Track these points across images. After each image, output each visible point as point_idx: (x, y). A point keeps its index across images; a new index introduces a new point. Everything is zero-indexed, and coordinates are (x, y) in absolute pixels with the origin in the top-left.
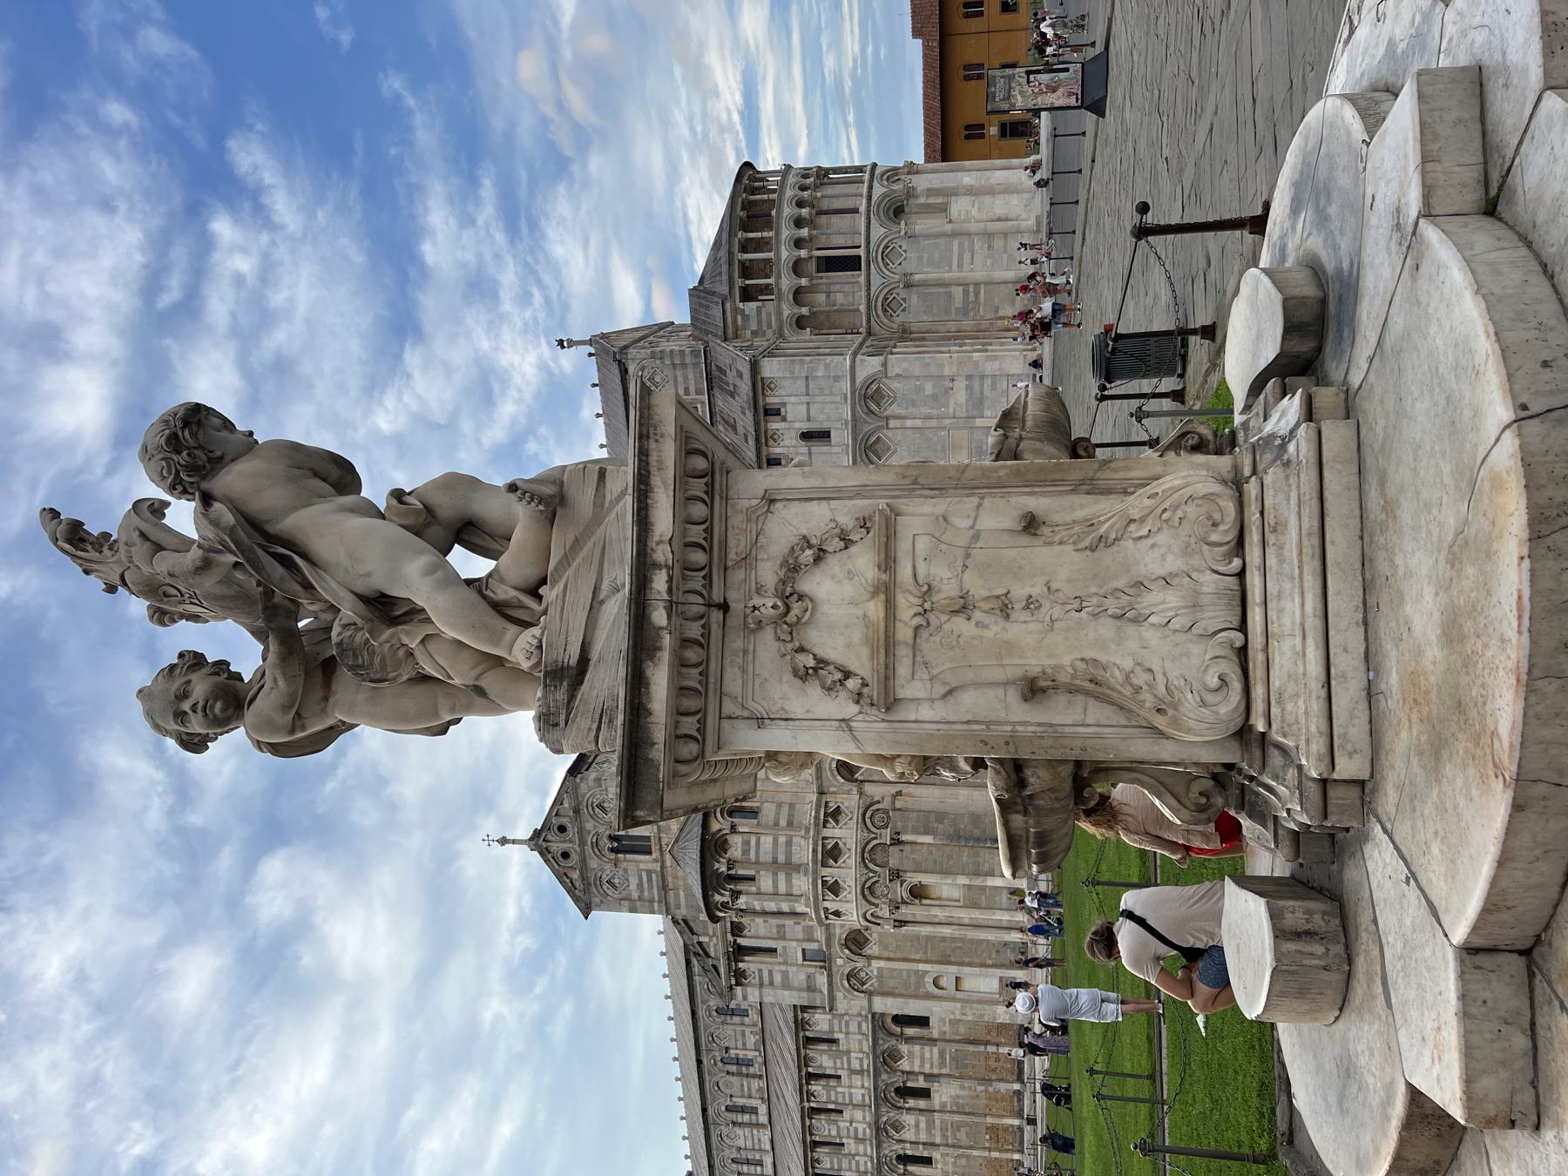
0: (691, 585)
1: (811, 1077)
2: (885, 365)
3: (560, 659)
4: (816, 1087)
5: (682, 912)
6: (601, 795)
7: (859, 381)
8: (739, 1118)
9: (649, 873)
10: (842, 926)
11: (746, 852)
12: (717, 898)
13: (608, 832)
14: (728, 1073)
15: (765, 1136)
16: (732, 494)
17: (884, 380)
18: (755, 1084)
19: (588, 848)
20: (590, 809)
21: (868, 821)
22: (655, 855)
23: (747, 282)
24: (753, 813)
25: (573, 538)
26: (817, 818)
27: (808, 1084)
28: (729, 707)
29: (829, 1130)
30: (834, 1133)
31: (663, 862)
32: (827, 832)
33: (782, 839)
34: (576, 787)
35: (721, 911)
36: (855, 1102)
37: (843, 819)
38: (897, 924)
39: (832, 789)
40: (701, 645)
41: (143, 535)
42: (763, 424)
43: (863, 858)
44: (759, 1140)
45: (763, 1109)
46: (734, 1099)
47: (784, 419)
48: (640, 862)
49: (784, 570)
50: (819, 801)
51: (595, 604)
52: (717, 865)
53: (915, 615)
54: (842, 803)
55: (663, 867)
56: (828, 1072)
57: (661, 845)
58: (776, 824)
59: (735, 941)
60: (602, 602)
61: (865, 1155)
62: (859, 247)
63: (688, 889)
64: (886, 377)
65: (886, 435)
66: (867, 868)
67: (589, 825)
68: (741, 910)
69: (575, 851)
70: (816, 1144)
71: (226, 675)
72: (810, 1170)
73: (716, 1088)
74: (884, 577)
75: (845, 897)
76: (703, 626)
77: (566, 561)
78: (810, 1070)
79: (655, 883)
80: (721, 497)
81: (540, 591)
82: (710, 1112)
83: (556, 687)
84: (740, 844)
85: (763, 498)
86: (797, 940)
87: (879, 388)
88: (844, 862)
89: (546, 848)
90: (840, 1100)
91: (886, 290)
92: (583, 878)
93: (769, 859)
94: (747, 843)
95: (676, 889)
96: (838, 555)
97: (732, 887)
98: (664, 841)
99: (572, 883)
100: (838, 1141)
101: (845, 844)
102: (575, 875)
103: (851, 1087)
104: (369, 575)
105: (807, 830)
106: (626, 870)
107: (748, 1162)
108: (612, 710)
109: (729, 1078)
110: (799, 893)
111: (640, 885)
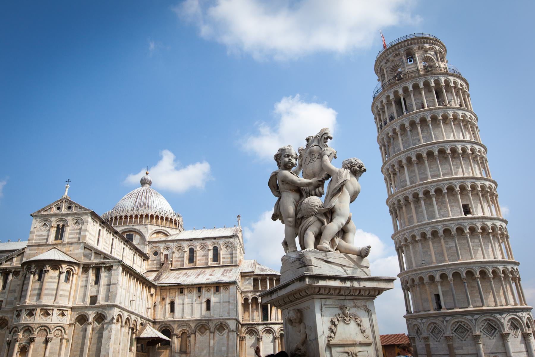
0: (352, 291)
2: (233, 331)
5: (27, 251)
7: (228, 322)
11: (51, 278)
12: (33, 266)
16: (369, 301)
17: (227, 331)
19: (61, 217)
20: (76, 218)
21: (58, 328)
23: (259, 280)
24: (67, 280)
26: (62, 307)
32: (55, 310)
34: (86, 214)
35: (27, 267)
37: (60, 317)
38: (9, 341)
40: (338, 294)
42: (213, 286)
43: (42, 326)
47: (214, 293)
52: (47, 266)
53: (351, 352)
59: (11, 272)
60: (342, 267)
62: (271, 321)
63: (37, 254)
64: (229, 332)
65: (208, 333)
66: (38, 328)
68: (26, 276)
74: (358, 344)
79: (42, 241)
86: (7, 298)
87: (225, 329)
88: (42, 318)
91: (257, 331)
94: (55, 278)
96: (360, 330)
97: (37, 272)
99: (47, 210)
111: (42, 235)
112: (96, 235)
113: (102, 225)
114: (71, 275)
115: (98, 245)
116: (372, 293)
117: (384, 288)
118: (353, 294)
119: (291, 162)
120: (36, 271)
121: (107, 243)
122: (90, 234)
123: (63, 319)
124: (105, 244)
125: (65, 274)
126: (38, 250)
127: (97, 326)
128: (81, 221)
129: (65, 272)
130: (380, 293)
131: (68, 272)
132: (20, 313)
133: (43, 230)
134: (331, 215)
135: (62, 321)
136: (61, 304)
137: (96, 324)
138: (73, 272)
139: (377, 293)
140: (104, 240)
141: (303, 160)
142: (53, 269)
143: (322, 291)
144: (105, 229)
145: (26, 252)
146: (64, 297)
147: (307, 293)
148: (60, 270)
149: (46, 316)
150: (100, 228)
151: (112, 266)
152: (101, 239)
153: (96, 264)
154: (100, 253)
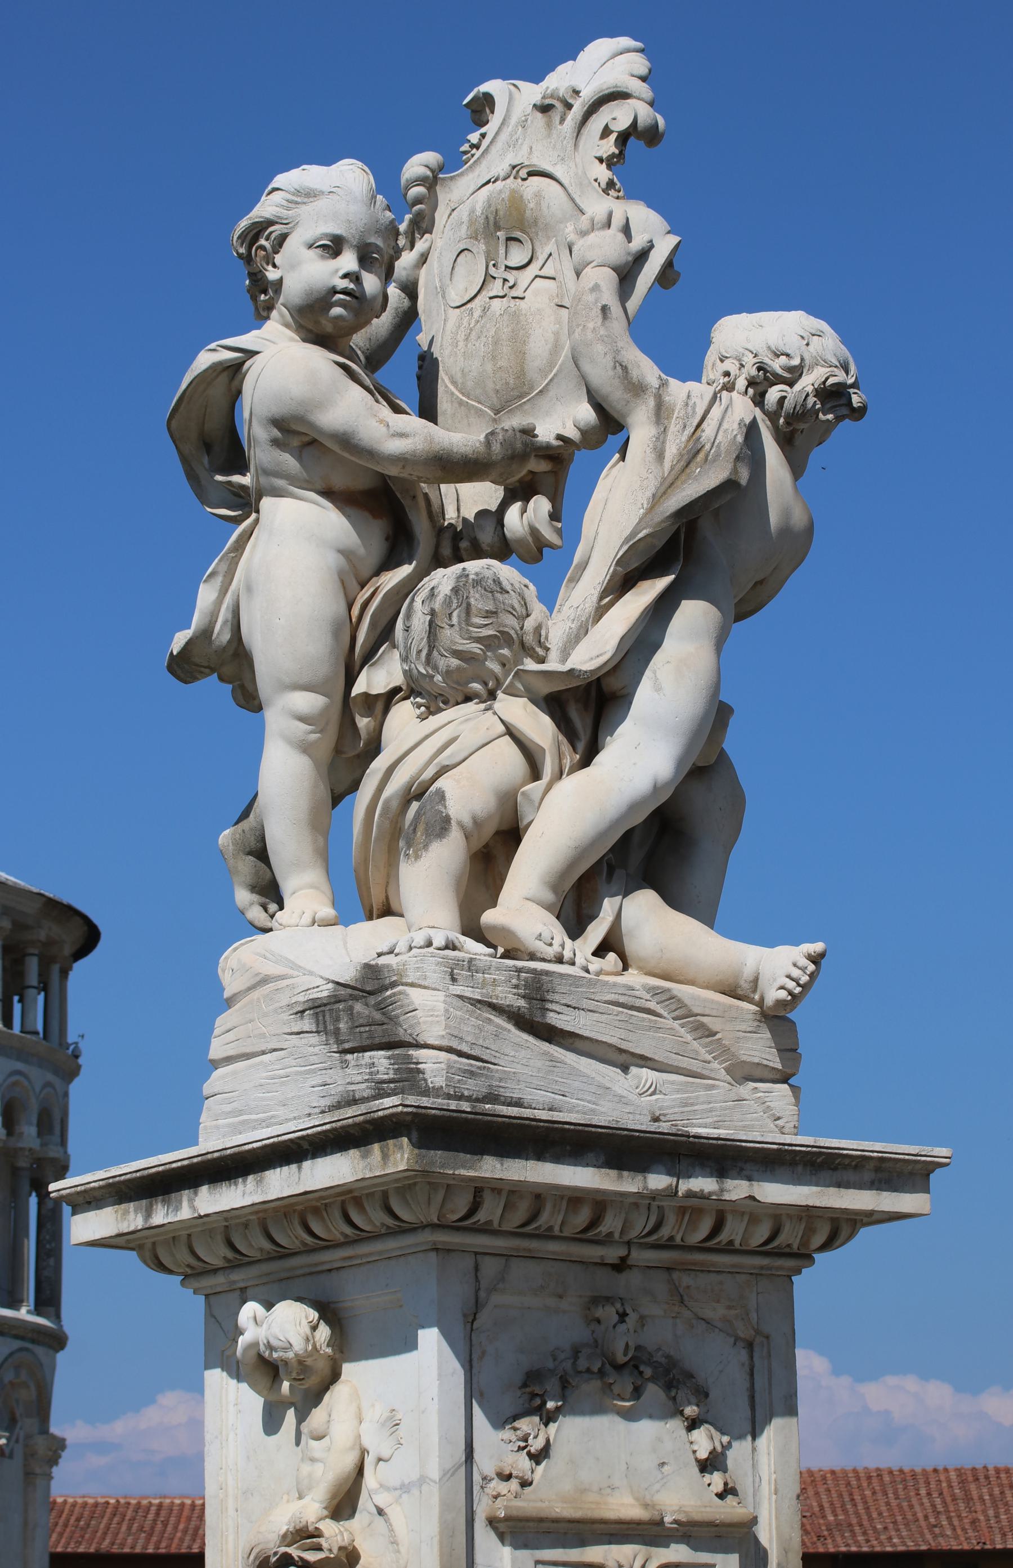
0: (671, 1219)
3: (556, 997)
25: (715, 1028)
28: (490, 1267)
40: (585, 1230)
49: (663, 1360)
51: (622, 1058)
60: (625, 1069)
76: (610, 1234)
77: (684, 1013)
80: (762, 1268)
83: (516, 987)
85: (758, 1332)
108: (487, 1077)
116: (790, 1236)
117: (870, 1213)
118: (671, 1238)
130: (844, 1233)
134: (589, 721)
139: (818, 1240)
141: (433, 258)
143: (490, 1211)
147: (396, 1217)
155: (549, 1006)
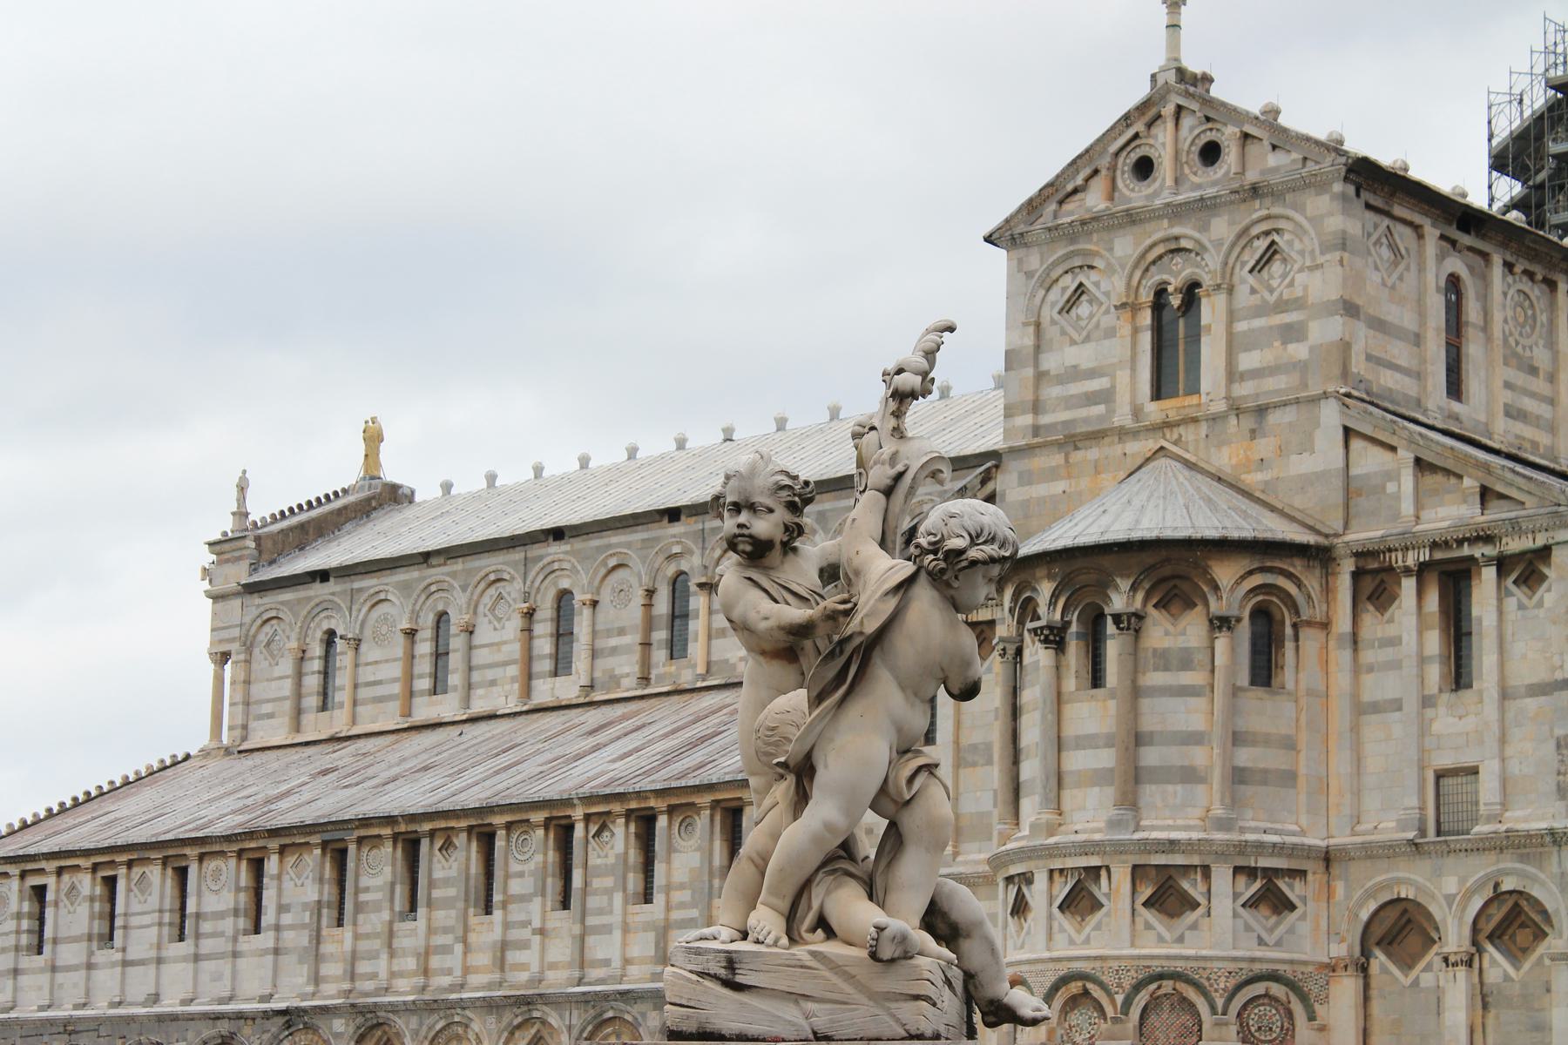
1: (645, 823)
4: (621, 838)
6: (1302, 253)
8: (544, 629)
9: (1106, 397)
10: (993, 917)
11: (1165, 661)
12: (1045, 589)
13: (1207, 281)
14: (650, 593)
15: (504, 698)
18: (627, 667)
19: (1163, 229)
20: (1264, 227)
21: (1258, 989)
22: (1155, 411)
24: (1264, 671)
26: (1260, 847)
27: (628, 815)
29: (521, 875)
30: (515, 887)
31: (1134, 434)
32: (1222, 877)
33: (1199, 756)
34: (1316, 184)
36: (591, 940)
37: (1260, 920)
39: (1339, 888)
41: (900, 475)
43: (1161, 977)
44: (493, 683)
45: (566, 690)
46: (587, 612)
48: (1133, 369)
50: (1307, 852)
51: (793, 996)
52: (1124, 584)
54: (1303, 917)
55: (1123, 433)
56: (659, 868)
57: (1177, 424)
58: (1237, 739)
60: (796, 1002)
61: (466, 970)
67: (1222, 228)
68: (1019, 652)
69: (1156, 194)
70: (487, 839)
71: (785, 539)
72: (427, 827)
73: (612, 562)
75: (1062, 930)
78: (662, 821)
79: (1082, 413)
81: (819, 931)
82: (555, 549)
84: (1181, 642)
88: (1148, 926)
89: (1159, 116)
90: (593, 902)
92: (1088, 224)
93: (1148, 724)
94: (1185, 661)
95: (1069, 471)
97: (1074, 628)
98: (1189, 433)
99: (1075, 191)
100: (497, 897)
101: (1194, 927)
102: (1094, 200)
103: (626, 929)
104: (826, 766)
105: (1224, 824)
106: (1111, 333)
107: (440, 655)
109: (639, 598)
110: (1067, 804)
111: (1075, 374)
112: (1422, 315)
113: (1466, 240)
114: (1289, 631)
115: (1455, 388)
119: (743, 535)
120: (1066, 625)
121: (1533, 371)
122: (1379, 325)
123: (1282, 929)
124: (1520, 378)
125: (1244, 630)
126: (1069, 477)
127: (1507, 978)
128: (1297, 245)
129: (1246, 614)
131: (1262, 615)
132: (1025, 889)
133: (1076, 336)
135: (1278, 944)
136: (1255, 830)
137: (1496, 963)
138: (1297, 613)
140: (1499, 353)
142: (1162, 605)
144: (1497, 270)
145: (1004, 495)
146: (1264, 782)
148: (1207, 604)
149: (1173, 914)
150: (1456, 264)
151: (1544, 553)
152: (1473, 349)
153: (1434, 545)
154: (1450, 464)
155: (737, 971)
